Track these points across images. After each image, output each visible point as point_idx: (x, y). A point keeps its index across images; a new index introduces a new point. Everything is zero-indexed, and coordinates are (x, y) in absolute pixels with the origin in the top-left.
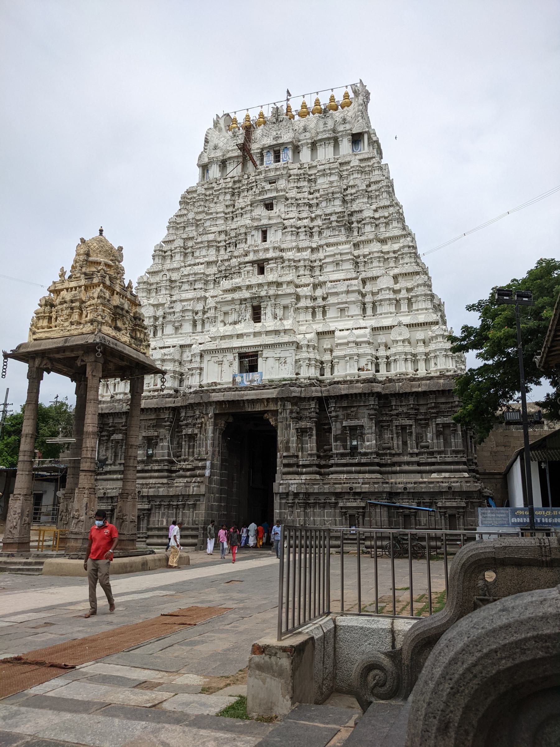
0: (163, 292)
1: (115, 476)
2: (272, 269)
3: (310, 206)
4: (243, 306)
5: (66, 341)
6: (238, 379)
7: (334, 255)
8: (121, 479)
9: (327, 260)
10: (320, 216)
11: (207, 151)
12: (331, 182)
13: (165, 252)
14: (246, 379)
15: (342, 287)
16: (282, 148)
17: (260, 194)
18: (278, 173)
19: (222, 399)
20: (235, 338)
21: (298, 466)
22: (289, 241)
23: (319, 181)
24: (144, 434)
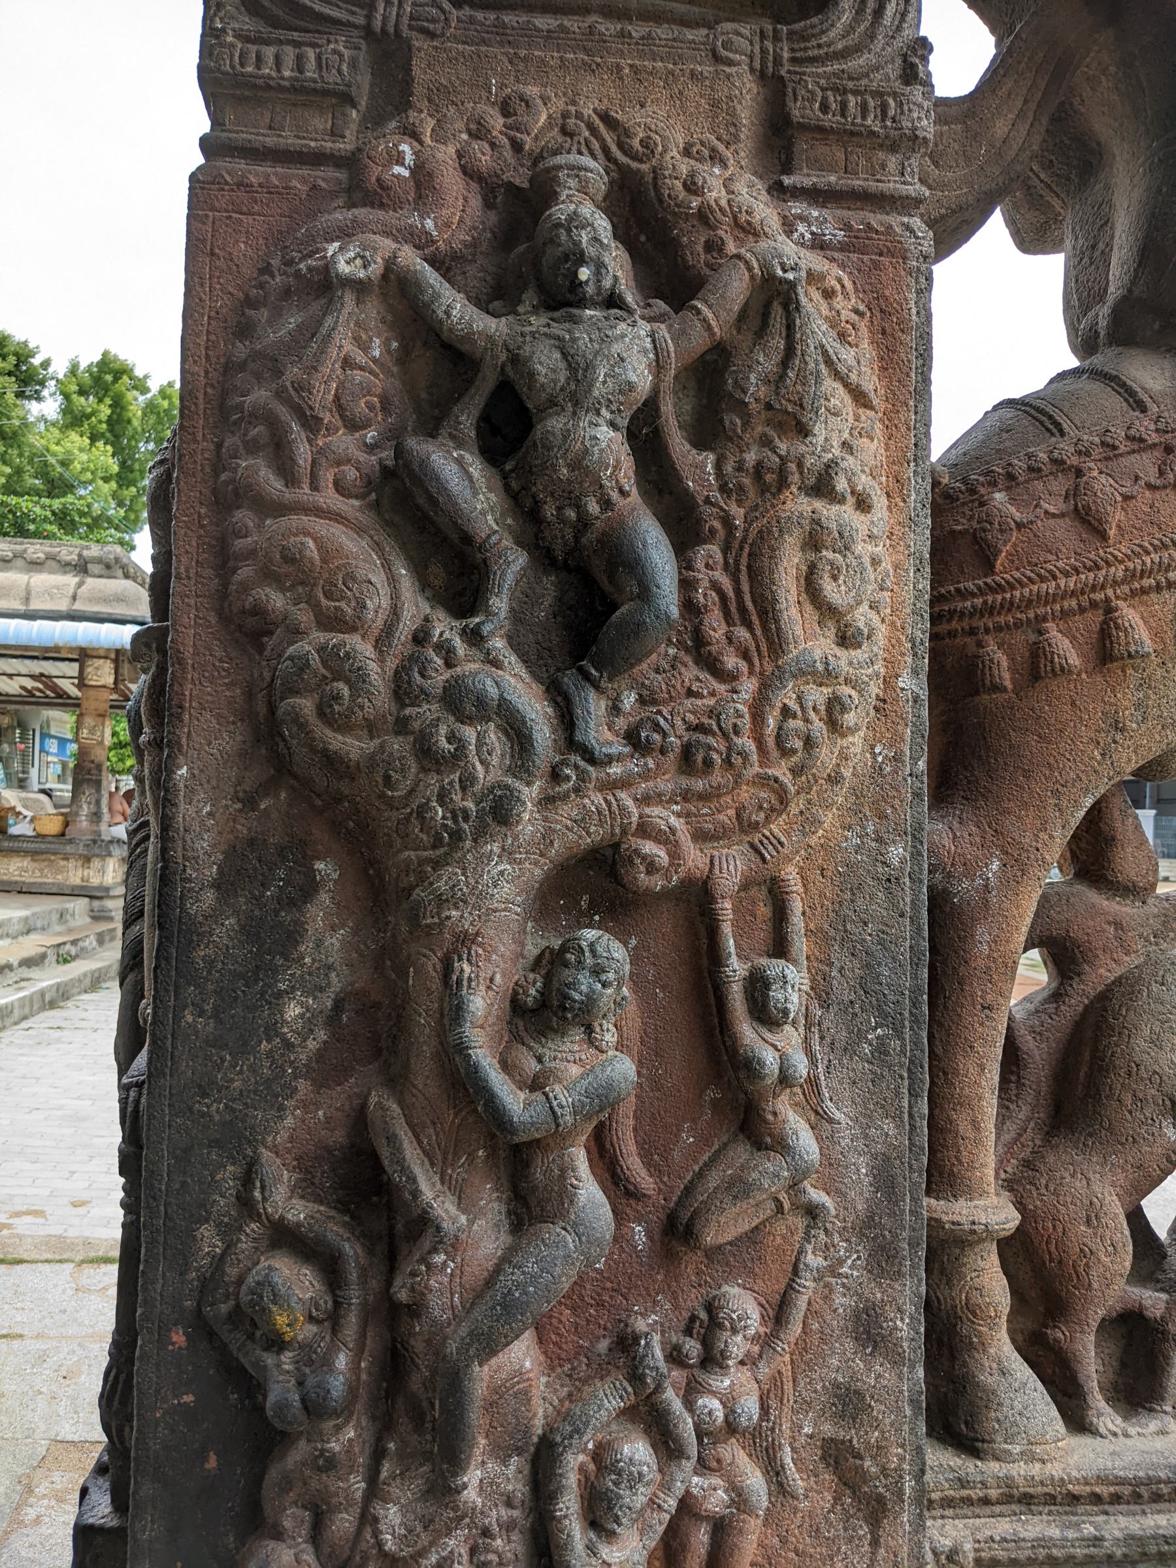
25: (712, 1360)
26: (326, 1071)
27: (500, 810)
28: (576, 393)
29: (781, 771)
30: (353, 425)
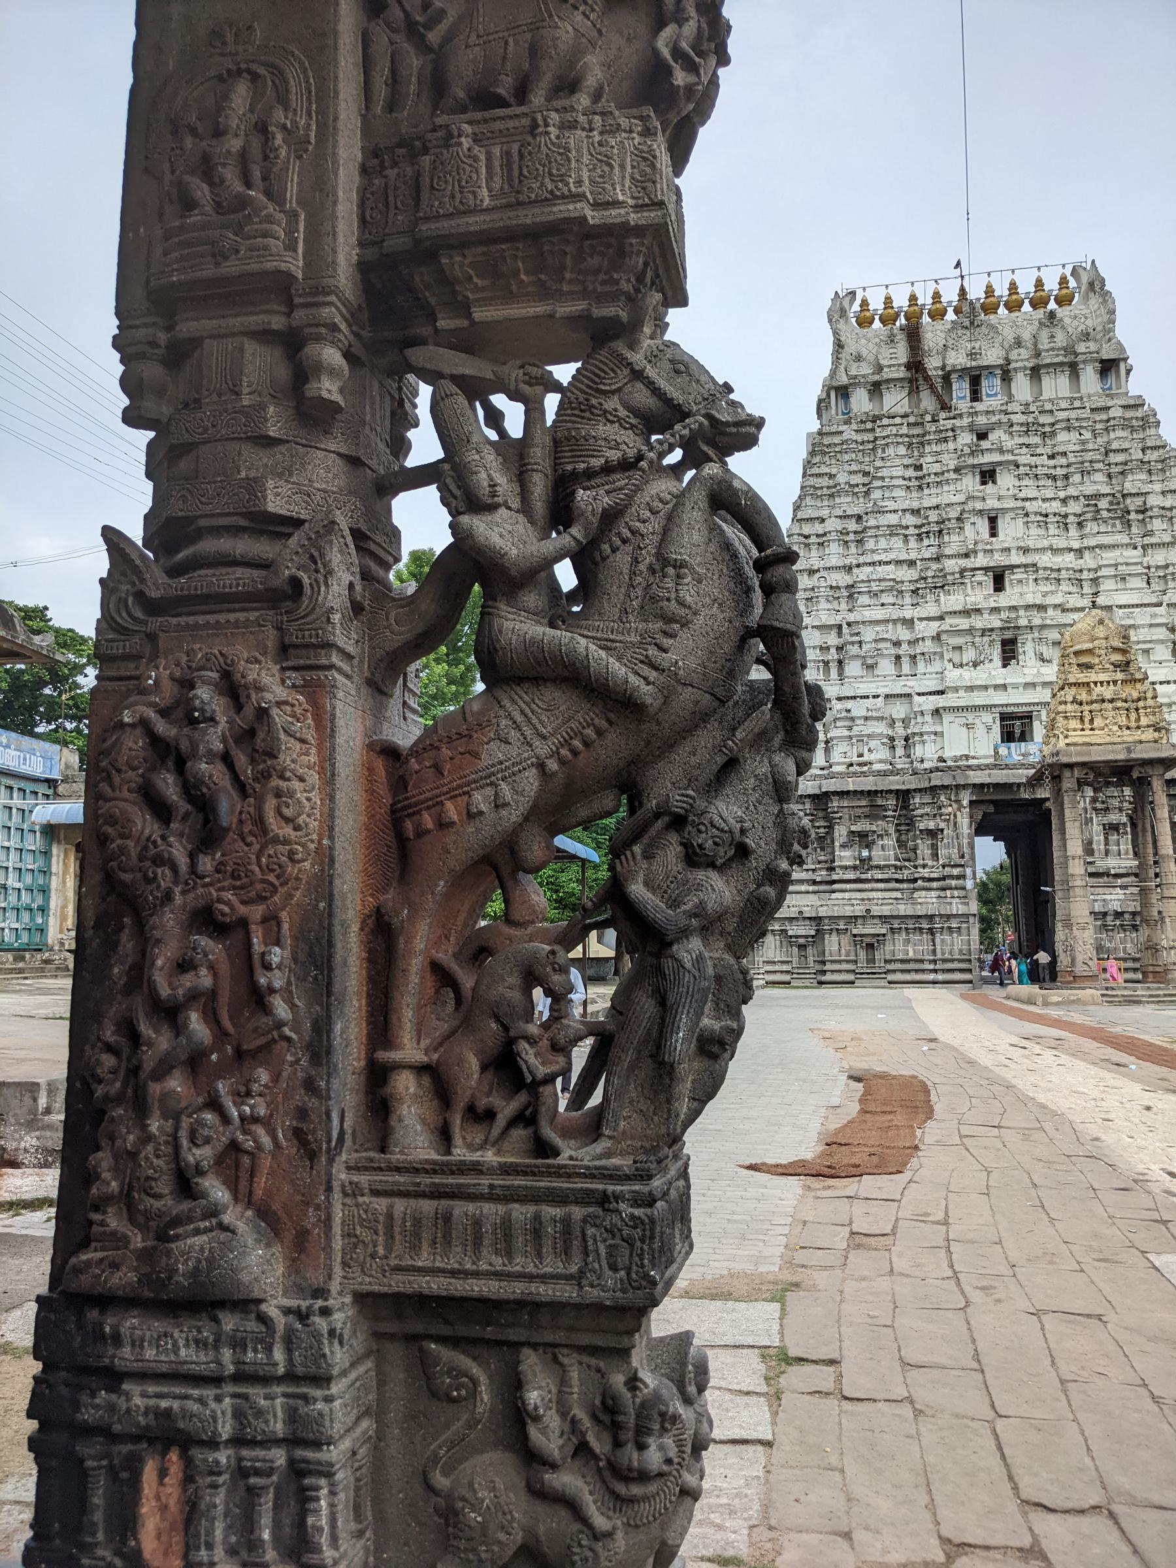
0: (823, 605)
1: (803, 888)
2: (1020, 581)
3: (1054, 478)
4: (986, 639)
5: (1129, 750)
6: (1003, 751)
7: (1116, 565)
8: (814, 892)
9: (1104, 572)
10: (1076, 498)
11: (844, 362)
12: (1083, 443)
13: (807, 537)
14: (1014, 752)
15: (1141, 617)
16: (985, 373)
17: (972, 453)
18: (994, 419)
19: (988, 780)
20: (991, 691)
21: (1108, 875)
22: (1035, 537)
23: (1062, 436)
24: (853, 828)
25: (248, 1094)
26: (128, 991)
27: (168, 897)
28: (194, 755)
29: (271, 877)
30: (133, 769)
